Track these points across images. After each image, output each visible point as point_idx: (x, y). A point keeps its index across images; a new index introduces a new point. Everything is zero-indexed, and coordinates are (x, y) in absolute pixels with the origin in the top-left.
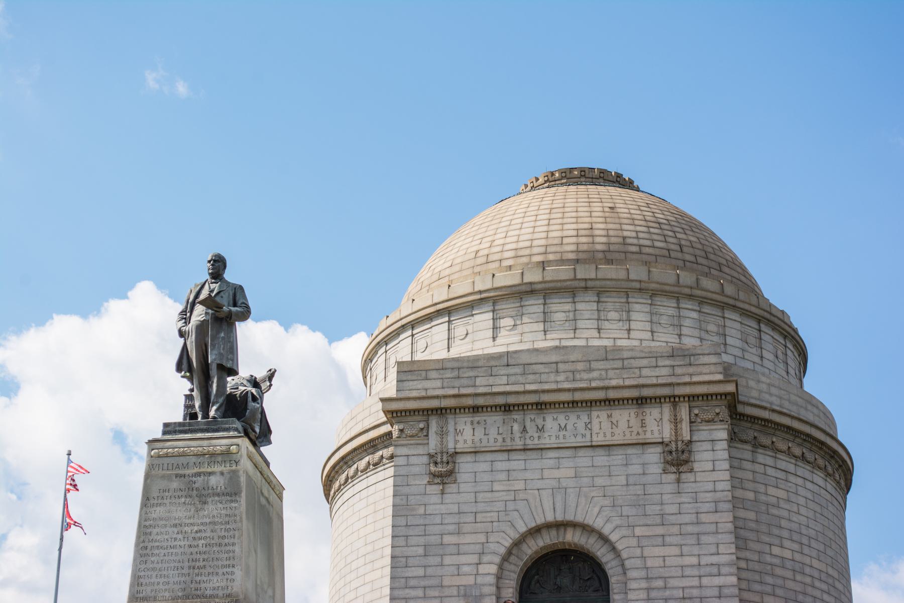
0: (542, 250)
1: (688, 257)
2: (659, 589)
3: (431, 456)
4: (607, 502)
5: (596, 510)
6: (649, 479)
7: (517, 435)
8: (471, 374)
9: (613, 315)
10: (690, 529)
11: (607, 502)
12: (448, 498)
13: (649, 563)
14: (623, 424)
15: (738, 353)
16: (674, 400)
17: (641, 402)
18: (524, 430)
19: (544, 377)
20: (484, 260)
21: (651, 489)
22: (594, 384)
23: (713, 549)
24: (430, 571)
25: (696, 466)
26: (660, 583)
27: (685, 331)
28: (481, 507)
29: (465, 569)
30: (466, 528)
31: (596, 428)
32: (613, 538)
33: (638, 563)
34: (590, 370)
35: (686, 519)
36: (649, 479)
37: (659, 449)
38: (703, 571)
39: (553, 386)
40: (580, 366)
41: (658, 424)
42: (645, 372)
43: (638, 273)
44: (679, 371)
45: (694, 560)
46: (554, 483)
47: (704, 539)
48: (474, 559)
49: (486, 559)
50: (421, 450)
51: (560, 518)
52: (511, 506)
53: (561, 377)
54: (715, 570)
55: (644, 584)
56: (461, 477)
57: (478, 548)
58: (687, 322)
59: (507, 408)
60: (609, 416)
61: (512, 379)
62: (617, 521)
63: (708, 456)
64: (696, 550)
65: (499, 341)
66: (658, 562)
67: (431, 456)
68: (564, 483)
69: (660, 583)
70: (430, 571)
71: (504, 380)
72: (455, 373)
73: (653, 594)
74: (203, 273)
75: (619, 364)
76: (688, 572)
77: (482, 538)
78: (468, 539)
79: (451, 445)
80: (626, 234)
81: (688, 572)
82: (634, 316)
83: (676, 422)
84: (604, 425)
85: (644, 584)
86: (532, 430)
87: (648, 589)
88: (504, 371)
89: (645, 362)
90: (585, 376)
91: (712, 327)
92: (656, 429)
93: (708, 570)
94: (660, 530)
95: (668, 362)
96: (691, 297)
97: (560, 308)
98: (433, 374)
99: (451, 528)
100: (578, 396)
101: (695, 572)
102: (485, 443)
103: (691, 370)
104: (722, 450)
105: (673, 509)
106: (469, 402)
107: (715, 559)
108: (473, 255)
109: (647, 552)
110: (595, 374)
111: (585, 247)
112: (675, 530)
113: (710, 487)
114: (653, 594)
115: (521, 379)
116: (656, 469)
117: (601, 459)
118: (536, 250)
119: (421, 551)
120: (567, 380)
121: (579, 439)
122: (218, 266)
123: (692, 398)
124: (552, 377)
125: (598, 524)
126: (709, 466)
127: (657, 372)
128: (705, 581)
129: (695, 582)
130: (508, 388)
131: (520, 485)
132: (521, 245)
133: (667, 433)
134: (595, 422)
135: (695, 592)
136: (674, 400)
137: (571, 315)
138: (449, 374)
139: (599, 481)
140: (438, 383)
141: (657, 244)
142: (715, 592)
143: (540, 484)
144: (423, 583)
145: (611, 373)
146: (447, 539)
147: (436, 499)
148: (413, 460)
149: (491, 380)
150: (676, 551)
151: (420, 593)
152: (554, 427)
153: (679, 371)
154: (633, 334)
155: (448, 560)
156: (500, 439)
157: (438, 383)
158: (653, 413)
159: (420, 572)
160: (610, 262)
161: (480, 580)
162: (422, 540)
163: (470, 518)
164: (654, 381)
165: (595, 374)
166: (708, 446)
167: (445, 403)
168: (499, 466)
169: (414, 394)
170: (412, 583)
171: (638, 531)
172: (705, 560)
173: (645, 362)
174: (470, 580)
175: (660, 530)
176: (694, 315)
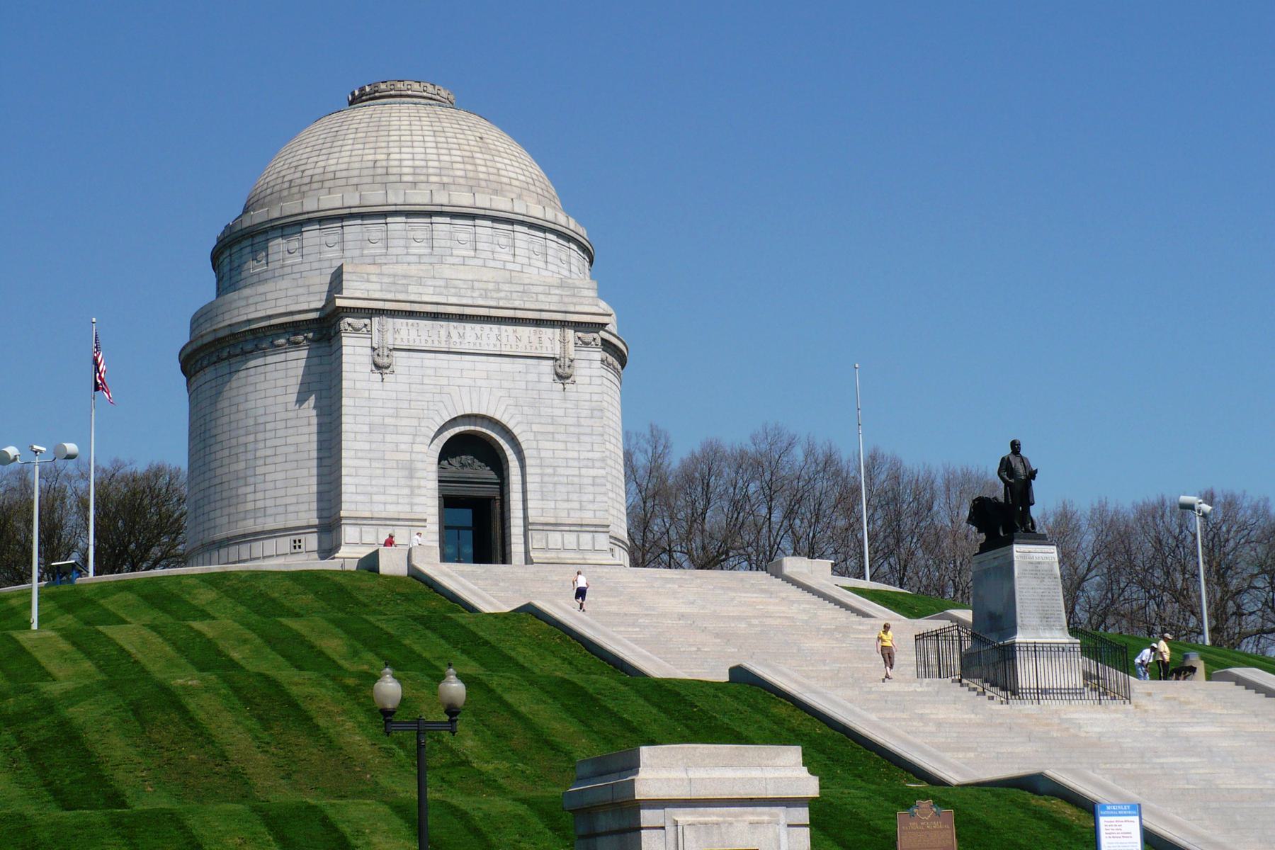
0: (437, 171)
1: (539, 191)
2: (550, 475)
3: (374, 349)
4: (512, 402)
5: (503, 408)
6: (542, 386)
7: (444, 338)
8: (404, 282)
9: (503, 241)
10: (572, 429)
11: (512, 402)
12: (387, 386)
13: (543, 454)
14: (525, 340)
15: (525, 261)
16: (563, 324)
17: (538, 323)
18: (449, 335)
19: (463, 292)
20: (384, 171)
21: (545, 395)
22: (501, 304)
23: (589, 448)
24: (374, 446)
25: (577, 379)
26: (550, 471)
27: (550, 259)
28: (414, 396)
29: (403, 447)
30: (402, 413)
31: (504, 340)
32: (516, 431)
33: (535, 453)
34: (499, 290)
35: (572, 421)
36: (542, 386)
37: (551, 362)
38: (582, 464)
39: (470, 302)
40: (491, 286)
41: (549, 340)
42: (541, 297)
43: (519, 208)
44: (566, 300)
45: (575, 455)
46: (471, 382)
47: (583, 438)
48: (408, 439)
49: (418, 439)
50: (368, 343)
51: (475, 412)
52: (437, 398)
53: (476, 294)
54: (590, 464)
55: (538, 471)
56: (398, 369)
57: (412, 430)
58: (550, 252)
59: (435, 316)
60: (515, 331)
61: (438, 290)
62: (518, 418)
63: (587, 372)
64: (576, 447)
65: (412, 251)
66: (549, 454)
67: (374, 349)
68: (479, 383)
69: (550, 471)
70: (374, 446)
71: (431, 290)
72: (391, 280)
73: (546, 479)
74: (1007, 451)
75: (520, 288)
76: (571, 463)
77: (415, 422)
78: (404, 422)
79: (390, 342)
80: (499, 165)
81: (571, 463)
82: (518, 243)
83: (563, 342)
84: (511, 338)
85: (538, 471)
86: (455, 337)
87: (542, 475)
88: (430, 282)
89: (540, 289)
90: (495, 295)
91: (564, 257)
92: (549, 346)
93: (585, 462)
94: (550, 428)
95: (557, 292)
96: (553, 231)
97: (463, 229)
98: (373, 278)
99: (391, 411)
100: (494, 313)
101: (575, 464)
102: (417, 343)
103: (575, 300)
104: (597, 370)
105: (561, 412)
106: (407, 307)
107: (590, 455)
108: (371, 164)
109: (543, 444)
110: (502, 295)
111: (471, 174)
112: (562, 429)
113: (587, 397)
114: (546, 479)
115: (445, 291)
116: (549, 377)
117: (507, 364)
118: (431, 171)
119: (366, 428)
120: (481, 296)
121: (491, 348)
122: (1015, 447)
123: (577, 326)
124: (469, 293)
125: (505, 419)
126: (587, 380)
127: (549, 299)
128: (583, 471)
129: (576, 472)
130: (435, 299)
131: (445, 382)
132: (417, 163)
133: (557, 352)
134: (504, 334)
135: (576, 480)
136: (563, 324)
137: (472, 237)
138: (386, 280)
139: (505, 384)
140: (378, 286)
141: (522, 178)
142: (590, 481)
143: (459, 382)
144: (369, 456)
145: (515, 295)
146: (387, 421)
147: (378, 385)
148: (358, 350)
149: (421, 290)
150: (561, 446)
151: (366, 463)
152: (471, 335)
153: (566, 300)
154: (518, 259)
155: (388, 438)
156: (430, 340)
157: (378, 286)
158: (547, 332)
159: (367, 446)
160: (496, 192)
161: (414, 456)
162: (367, 420)
163: (406, 405)
164: (547, 308)
165: (502, 295)
166: (585, 364)
167: (388, 306)
168: (427, 363)
169: (358, 294)
170: (360, 454)
171: (535, 428)
172: (584, 455)
173: (540, 289)
174: (407, 456)
175: (550, 428)
176: (554, 245)
